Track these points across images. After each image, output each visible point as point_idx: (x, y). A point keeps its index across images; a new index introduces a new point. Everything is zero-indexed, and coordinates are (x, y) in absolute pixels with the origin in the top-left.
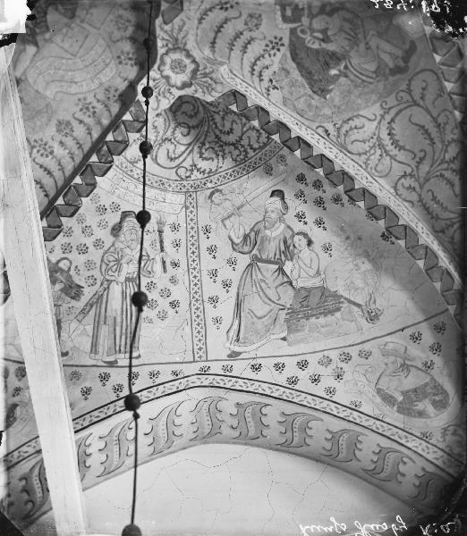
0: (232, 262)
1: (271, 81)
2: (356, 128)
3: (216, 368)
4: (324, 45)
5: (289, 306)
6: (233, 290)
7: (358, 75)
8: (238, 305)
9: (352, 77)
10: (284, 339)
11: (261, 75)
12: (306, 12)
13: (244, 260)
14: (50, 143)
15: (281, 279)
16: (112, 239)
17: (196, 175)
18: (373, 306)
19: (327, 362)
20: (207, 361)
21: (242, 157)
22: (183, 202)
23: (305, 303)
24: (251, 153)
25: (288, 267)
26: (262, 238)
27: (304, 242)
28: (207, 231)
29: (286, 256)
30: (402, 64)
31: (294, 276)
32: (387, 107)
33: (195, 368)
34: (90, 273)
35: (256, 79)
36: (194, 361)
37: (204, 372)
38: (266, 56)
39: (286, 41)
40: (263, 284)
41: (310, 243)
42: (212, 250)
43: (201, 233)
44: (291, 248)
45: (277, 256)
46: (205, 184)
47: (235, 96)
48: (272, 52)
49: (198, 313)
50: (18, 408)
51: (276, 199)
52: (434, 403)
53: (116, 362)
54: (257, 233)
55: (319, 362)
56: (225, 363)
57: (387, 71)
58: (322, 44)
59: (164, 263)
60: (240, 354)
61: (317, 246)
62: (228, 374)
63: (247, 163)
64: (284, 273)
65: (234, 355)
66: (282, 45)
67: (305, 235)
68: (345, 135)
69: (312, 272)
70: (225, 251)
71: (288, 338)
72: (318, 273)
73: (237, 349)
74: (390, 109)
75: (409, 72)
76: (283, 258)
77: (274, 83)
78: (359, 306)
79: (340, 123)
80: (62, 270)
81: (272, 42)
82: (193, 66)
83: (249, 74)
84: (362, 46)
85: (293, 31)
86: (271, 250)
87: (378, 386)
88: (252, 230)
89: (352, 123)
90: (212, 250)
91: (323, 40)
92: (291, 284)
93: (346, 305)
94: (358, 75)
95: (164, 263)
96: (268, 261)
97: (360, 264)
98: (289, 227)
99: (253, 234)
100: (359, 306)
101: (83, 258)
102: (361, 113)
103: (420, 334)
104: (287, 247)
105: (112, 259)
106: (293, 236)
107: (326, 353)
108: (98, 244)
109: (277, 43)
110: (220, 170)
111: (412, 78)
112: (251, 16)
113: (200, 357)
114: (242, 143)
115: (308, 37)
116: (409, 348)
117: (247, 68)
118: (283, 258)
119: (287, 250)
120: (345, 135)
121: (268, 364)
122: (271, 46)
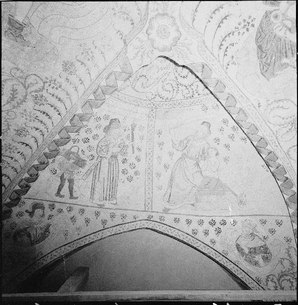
0: (171, 154)
1: (233, 57)
2: (282, 107)
3: (156, 217)
6: (169, 171)
8: (172, 180)
10: (193, 205)
11: (226, 51)
14: (59, 80)
15: (196, 169)
16: (104, 134)
17: (158, 99)
19: (213, 223)
21: (189, 95)
25: (202, 163)
27: (215, 153)
28: (160, 133)
29: (201, 157)
33: (145, 216)
34: (90, 153)
35: (222, 53)
36: (145, 211)
37: (149, 219)
38: (236, 34)
41: (217, 154)
50: (51, 226)
51: (205, 127)
52: (263, 258)
53: (103, 205)
54: (188, 142)
56: (161, 215)
58: (288, 32)
59: (133, 148)
62: (162, 222)
65: (166, 211)
67: (215, 149)
71: (195, 205)
73: (167, 207)
76: (200, 158)
77: (234, 59)
78: (235, 195)
80: (73, 153)
81: (245, 21)
82: (176, 34)
83: (218, 48)
87: (237, 242)
89: (281, 104)
90: (161, 144)
92: (201, 173)
95: (133, 148)
98: (208, 143)
99: (185, 142)
101: (86, 145)
104: (203, 153)
105: (103, 144)
108: (96, 137)
109: (249, 23)
114: (192, 87)
115: (277, 23)
116: (258, 226)
117: (217, 43)
118: (200, 158)
121: (183, 220)
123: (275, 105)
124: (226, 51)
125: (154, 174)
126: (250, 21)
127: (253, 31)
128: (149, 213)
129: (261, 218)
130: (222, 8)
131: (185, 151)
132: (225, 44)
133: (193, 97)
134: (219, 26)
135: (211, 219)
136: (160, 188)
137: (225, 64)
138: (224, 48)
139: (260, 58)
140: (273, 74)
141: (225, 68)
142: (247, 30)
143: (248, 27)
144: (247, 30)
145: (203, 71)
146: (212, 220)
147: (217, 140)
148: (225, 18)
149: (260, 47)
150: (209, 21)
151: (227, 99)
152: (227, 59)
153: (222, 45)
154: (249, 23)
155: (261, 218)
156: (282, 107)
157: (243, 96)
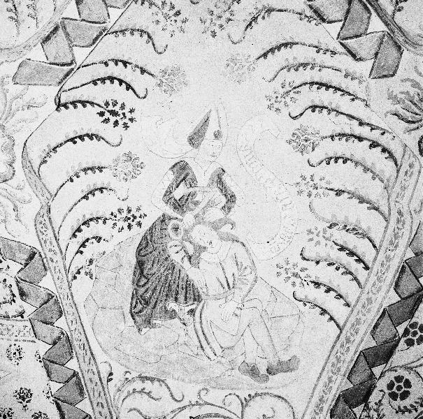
1: (91, 262)
4: (186, 263)
7: (200, 333)
9: (190, 328)
11: (83, 245)
12: (198, 210)
30: (263, 371)
32: (206, 399)
35: (74, 245)
39: (147, 223)
47: (32, 257)
48: (121, 224)
57: (241, 359)
66: (139, 224)
68: (129, 394)
74: (207, 403)
75: (263, 385)
77: (92, 267)
79: (135, 374)
81: (129, 211)
84: (231, 306)
85: (163, 220)
89: (148, 385)
91: (190, 258)
94: (200, 333)
102: (170, 382)
109: (135, 217)
111: (261, 395)
112: (129, 157)
120: (129, 394)
122: (125, 214)
123: (138, 385)
124: (83, 245)
126: (137, 215)
127: (137, 234)
130: (101, 171)
132: (87, 232)
134: (86, 197)
137: (73, 270)
138: (81, 237)
139: (136, 283)
140: (148, 322)
141: (70, 277)
142: (130, 227)
143: (132, 223)
144: (130, 227)
145: (26, 264)
148: (101, 190)
149: (140, 264)
150: (72, 181)
151: (55, 343)
152: (80, 261)
153: (79, 230)
154: (135, 217)
156: (148, 394)
157: (87, 347)
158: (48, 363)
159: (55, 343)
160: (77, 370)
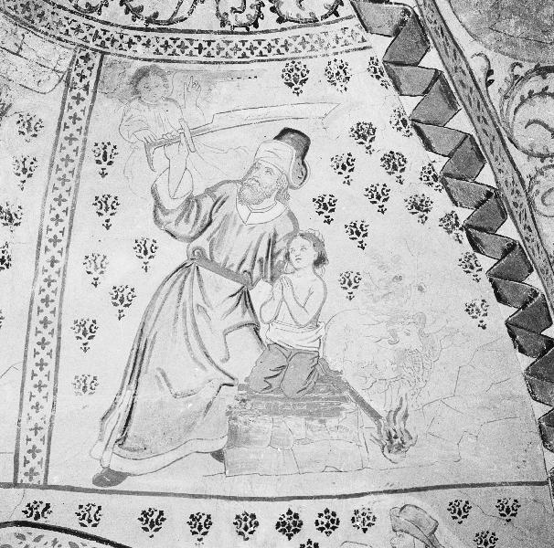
0: (145, 250)
5: (242, 381)
6: (134, 314)
8: (139, 356)
10: (219, 455)
13: (172, 253)
15: (240, 315)
18: (399, 426)
20: (46, 487)
21: (243, 18)
22: (64, 69)
23: (274, 382)
24: (269, 20)
25: (260, 293)
26: (226, 217)
27: (312, 255)
28: (105, 157)
31: (266, 315)
36: (15, 485)
40: (200, 319)
41: (320, 261)
42: (106, 205)
43: (90, 156)
44: (281, 257)
45: (246, 266)
46: (130, 43)
49: (41, 376)
51: (287, 150)
54: (219, 202)
55: (278, 525)
56: (85, 499)
60: (120, 476)
61: (331, 271)
62: (89, 530)
63: (250, 38)
64: (249, 304)
65: (109, 480)
67: (318, 243)
68: (523, 101)
69: (305, 318)
70: (135, 220)
71: (228, 455)
72: (315, 323)
73: (117, 464)
76: (256, 273)
78: (375, 415)
79: (528, 67)
86: (237, 245)
88: (209, 191)
92: (256, 330)
93: (350, 406)
96: (225, 271)
97: (401, 335)
98: (291, 216)
99: (207, 204)
100: (375, 415)
103: (467, 507)
104: (271, 254)
106: (291, 236)
107: (295, 506)
110: (179, 26)
113: (32, 473)
118: (256, 273)
119: (272, 260)
120: (523, 101)
125: (68, 324)
128: (34, 495)
129: (452, 495)
131: (202, 242)
133: (256, 25)
135: (283, 507)
136: (87, 385)
146: (290, 512)
147: (325, 206)
155: (452, 495)
157: (446, 33)
158: (392, 70)
159: (397, 32)
160: (441, 68)
